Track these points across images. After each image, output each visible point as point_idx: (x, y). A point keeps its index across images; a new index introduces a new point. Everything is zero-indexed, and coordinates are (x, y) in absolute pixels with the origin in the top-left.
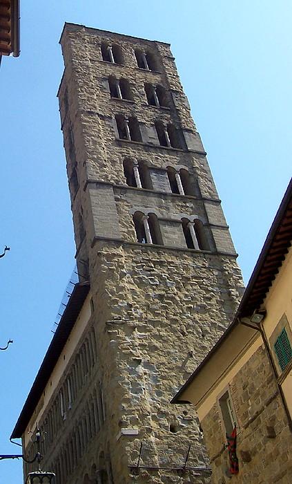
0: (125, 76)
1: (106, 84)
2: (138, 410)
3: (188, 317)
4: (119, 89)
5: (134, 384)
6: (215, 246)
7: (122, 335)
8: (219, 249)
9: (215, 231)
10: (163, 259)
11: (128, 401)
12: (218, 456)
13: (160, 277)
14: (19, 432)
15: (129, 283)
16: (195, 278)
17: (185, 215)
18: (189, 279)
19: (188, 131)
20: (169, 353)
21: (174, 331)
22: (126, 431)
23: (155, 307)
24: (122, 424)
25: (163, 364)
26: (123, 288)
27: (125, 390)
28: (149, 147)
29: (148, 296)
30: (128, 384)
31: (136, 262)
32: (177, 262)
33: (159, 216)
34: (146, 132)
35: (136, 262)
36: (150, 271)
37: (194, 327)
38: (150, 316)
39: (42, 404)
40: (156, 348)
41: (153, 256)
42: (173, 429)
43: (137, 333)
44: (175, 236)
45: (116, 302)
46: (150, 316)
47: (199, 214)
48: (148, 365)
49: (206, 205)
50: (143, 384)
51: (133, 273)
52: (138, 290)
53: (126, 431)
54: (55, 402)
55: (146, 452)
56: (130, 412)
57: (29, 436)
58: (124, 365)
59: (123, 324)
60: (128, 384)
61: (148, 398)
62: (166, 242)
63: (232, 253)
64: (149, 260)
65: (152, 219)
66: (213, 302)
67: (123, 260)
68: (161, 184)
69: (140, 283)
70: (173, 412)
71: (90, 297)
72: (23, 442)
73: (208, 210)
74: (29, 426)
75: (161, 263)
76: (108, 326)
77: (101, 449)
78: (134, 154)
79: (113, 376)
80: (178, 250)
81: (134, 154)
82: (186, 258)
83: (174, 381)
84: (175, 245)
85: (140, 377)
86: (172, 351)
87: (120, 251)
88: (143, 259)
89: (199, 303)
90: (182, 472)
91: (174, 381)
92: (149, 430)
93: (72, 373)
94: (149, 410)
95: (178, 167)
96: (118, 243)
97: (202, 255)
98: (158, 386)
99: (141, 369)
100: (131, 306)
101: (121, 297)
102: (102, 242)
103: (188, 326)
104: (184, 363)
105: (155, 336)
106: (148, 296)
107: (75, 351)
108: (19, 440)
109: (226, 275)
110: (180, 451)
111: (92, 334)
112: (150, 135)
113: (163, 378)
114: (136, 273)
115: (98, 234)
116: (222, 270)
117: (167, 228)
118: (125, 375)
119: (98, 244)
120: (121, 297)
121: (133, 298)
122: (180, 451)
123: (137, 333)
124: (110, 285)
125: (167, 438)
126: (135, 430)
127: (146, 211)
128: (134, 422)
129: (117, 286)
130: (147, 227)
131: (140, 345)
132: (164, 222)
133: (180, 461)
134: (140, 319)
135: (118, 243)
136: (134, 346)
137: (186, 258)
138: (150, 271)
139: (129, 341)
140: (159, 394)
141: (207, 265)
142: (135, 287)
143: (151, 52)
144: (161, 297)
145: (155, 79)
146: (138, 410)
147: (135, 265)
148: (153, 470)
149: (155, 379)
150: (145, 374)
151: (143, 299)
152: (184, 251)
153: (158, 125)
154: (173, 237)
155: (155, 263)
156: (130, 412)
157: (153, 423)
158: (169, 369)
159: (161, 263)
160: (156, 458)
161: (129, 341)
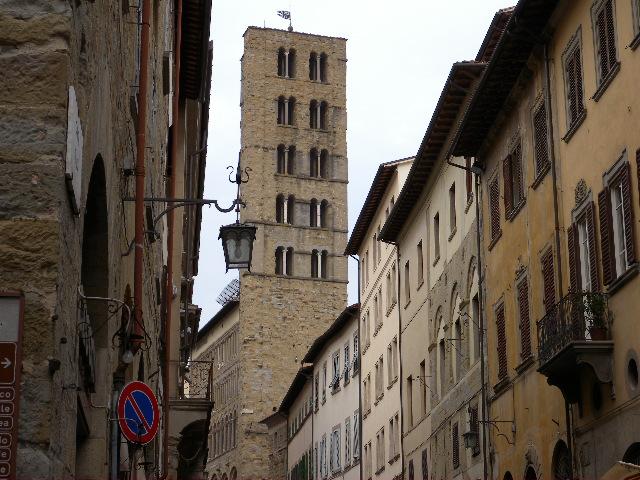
0: (295, 94)
1: (275, 106)
4: (286, 107)
19: (338, 156)
28: (301, 178)
32: (302, 289)
34: (301, 163)
41: (285, 285)
62: (296, 273)
65: (290, 251)
68: (302, 215)
78: (288, 187)
81: (288, 187)
84: (301, 275)
95: (319, 199)
112: (304, 164)
127: (286, 245)
143: (327, 53)
145: (320, 92)
153: (313, 153)
154: (302, 266)
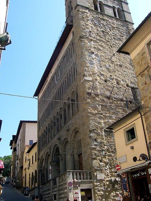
2: (92, 71)
3: (114, 41)
5: (91, 61)
6: (125, 19)
7: (87, 42)
8: (127, 20)
9: (125, 13)
10: (104, 18)
11: (88, 67)
12: (144, 71)
13: (103, 24)
14: (37, 94)
15: (90, 24)
16: (117, 28)
17: (114, 5)
18: (114, 28)
20: (105, 52)
21: (108, 45)
22: (86, 78)
23: (101, 35)
24: (84, 75)
25: (103, 56)
26: (88, 25)
27: (87, 63)
29: (98, 30)
30: (88, 60)
31: (94, 17)
32: (110, 21)
33: (104, 3)
35: (94, 17)
36: (99, 21)
37: (116, 45)
38: (98, 38)
39: (47, 81)
40: (100, 50)
41: (100, 16)
42: (106, 81)
43: (92, 42)
44: (110, 12)
45: (85, 29)
46: (98, 38)
47: (119, 6)
48: (96, 55)
49: (122, 3)
50: (94, 62)
51: (92, 21)
52: (94, 27)
53: (86, 78)
54: (53, 79)
55: (94, 88)
56: (89, 71)
57: (41, 95)
58: (86, 53)
59: (87, 38)
60: (88, 60)
61: (96, 68)
63: (131, 22)
64: (99, 18)
66: (124, 37)
67: (88, 15)
69: (95, 25)
70: (106, 75)
71: (72, 31)
72: (38, 97)
73: (123, 5)
74: (41, 92)
75: (104, 20)
76: (81, 37)
77: (72, 90)
79: (81, 57)
80: (111, 17)
82: (113, 20)
83: (107, 63)
84: (109, 14)
85: (93, 59)
86: (107, 52)
87: (87, 11)
88: (96, 16)
89: (118, 37)
90: (109, 98)
91: (107, 63)
92: (96, 80)
93: (61, 65)
94: (96, 72)
96: (87, 8)
97: (120, 21)
98: (100, 64)
99: (93, 56)
100: (91, 32)
101: (87, 28)
102: (80, 7)
103: (113, 44)
104: (111, 58)
105: (100, 45)
106: (98, 30)
107: (63, 55)
108: (37, 97)
109: (129, 29)
110: (109, 90)
111: (72, 45)
113: (103, 61)
114: (93, 21)
115: (78, 3)
116: (128, 28)
117: (106, 8)
118: (87, 57)
119: (78, 7)
120: (87, 28)
121: (92, 30)
122: (109, 90)
123: (92, 42)
124: (82, 23)
125: (103, 84)
126: (90, 79)
128: (90, 75)
129: (85, 24)
130: (98, 6)
131: (93, 47)
132: (105, 6)
133: (108, 94)
134: (94, 38)
135: (87, 8)
136: (91, 47)
137: (113, 20)
138: (99, 23)
139: (89, 44)
140: (101, 67)
141: (122, 24)
142: (93, 26)
144: (103, 32)
146: (92, 71)
147: (93, 18)
148: (97, 95)
149: (99, 61)
150: (95, 58)
151: (95, 31)
152: (113, 17)
154: (109, 12)
155: (101, 19)
156: (89, 71)
157: (97, 77)
158: (105, 58)
159: (104, 20)
160: (98, 91)
161: (89, 44)
